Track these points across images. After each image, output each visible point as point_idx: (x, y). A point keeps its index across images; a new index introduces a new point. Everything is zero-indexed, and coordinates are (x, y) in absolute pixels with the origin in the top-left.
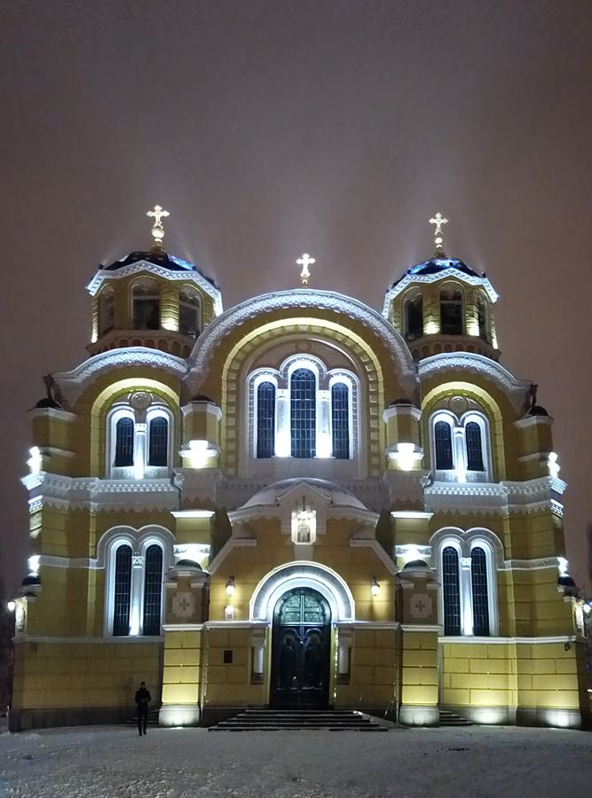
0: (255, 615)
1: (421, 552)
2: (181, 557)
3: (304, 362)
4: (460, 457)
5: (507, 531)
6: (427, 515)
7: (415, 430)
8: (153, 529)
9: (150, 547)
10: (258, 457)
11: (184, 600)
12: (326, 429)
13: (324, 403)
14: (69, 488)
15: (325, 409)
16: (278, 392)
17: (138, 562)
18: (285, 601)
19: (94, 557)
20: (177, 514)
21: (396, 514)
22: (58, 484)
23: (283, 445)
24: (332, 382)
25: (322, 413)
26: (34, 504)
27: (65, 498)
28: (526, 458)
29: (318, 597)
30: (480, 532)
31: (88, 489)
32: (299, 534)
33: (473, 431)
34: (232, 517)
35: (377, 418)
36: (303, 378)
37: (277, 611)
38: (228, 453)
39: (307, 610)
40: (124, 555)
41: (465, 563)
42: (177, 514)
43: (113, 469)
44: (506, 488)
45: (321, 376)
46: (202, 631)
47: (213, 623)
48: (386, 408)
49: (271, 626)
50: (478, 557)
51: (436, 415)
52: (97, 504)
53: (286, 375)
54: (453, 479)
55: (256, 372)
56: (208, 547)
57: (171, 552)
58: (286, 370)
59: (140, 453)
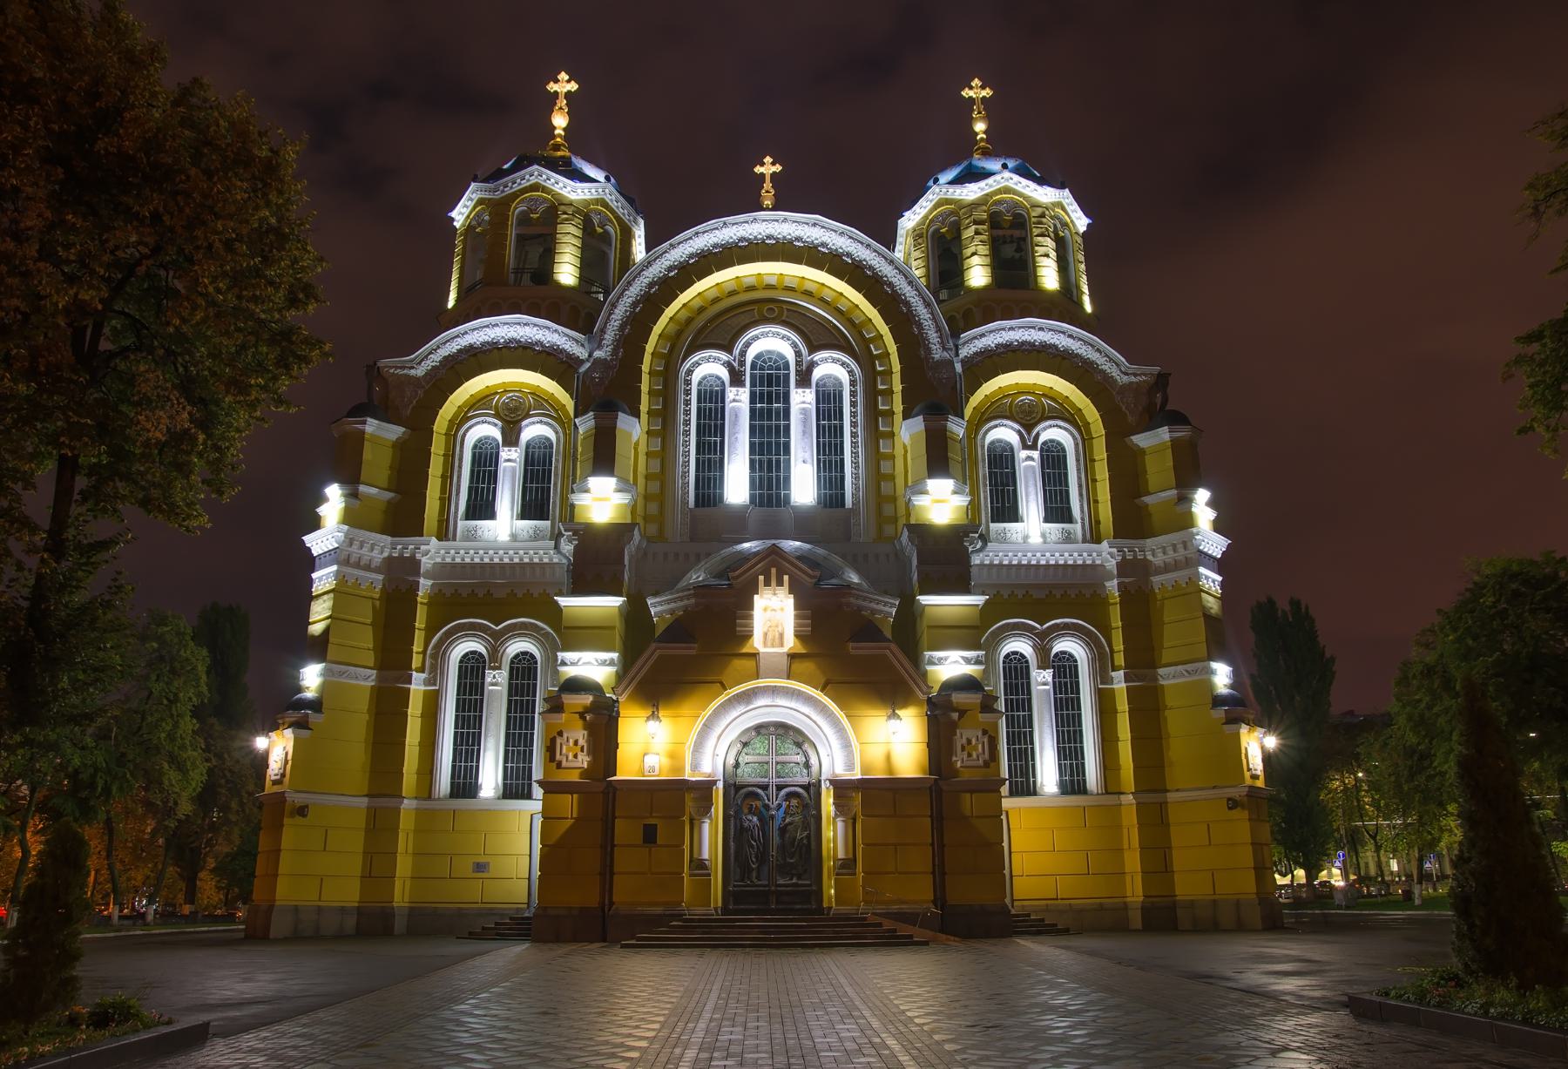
1: (968, 661)
2: (570, 672)
4: (1031, 505)
5: (1116, 622)
6: (977, 600)
7: (955, 455)
9: (517, 656)
10: (697, 504)
11: (576, 743)
12: (807, 456)
13: (805, 412)
14: (386, 554)
15: (805, 422)
16: (731, 393)
17: (497, 681)
18: (745, 744)
19: (421, 670)
20: (564, 601)
21: (926, 600)
22: (367, 547)
23: (737, 487)
24: (817, 373)
25: (800, 428)
26: (320, 579)
27: (377, 570)
28: (1146, 499)
30: (1066, 626)
31: (418, 556)
32: (766, 634)
33: (1053, 459)
34: (656, 607)
35: (892, 435)
36: (770, 368)
37: (731, 761)
38: (647, 498)
40: (473, 670)
41: (1042, 678)
42: (564, 601)
43: (462, 525)
44: (1115, 550)
45: (798, 363)
48: (906, 415)
49: (720, 785)
50: (1064, 668)
51: (996, 426)
52: (430, 583)
53: (742, 363)
54: (1020, 540)
55: (696, 358)
56: (615, 655)
57: (553, 664)
58: (743, 353)
59: (506, 500)
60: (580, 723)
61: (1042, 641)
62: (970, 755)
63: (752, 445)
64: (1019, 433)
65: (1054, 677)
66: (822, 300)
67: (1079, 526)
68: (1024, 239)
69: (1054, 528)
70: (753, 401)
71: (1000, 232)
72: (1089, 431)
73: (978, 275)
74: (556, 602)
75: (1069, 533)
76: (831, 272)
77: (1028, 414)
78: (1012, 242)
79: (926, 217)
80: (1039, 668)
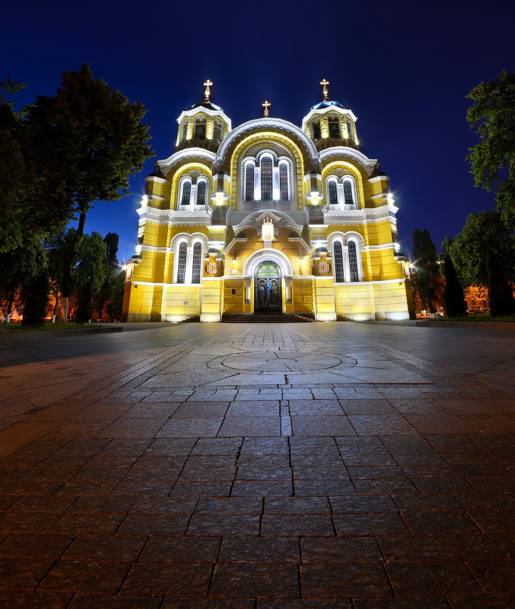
0: (246, 273)
1: (323, 243)
2: (211, 247)
3: (267, 154)
8: (198, 235)
10: (246, 200)
11: (213, 267)
12: (277, 186)
15: (277, 177)
16: (256, 169)
18: (260, 267)
25: (275, 178)
29: (275, 265)
33: (347, 187)
35: (301, 180)
37: (256, 272)
39: (270, 271)
41: (345, 249)
45: (274, 160)
46: (221, 281)
47: (227, 276)
48: (305, 174)
49: (253, 278)
53: (259, 160)
54: (338, 209)
58: (259, 158)
60: (214, 261)
61: (345, 238)
62: (324, 269)
63: (262, 183)
64: (337, 179)
65: (349, 248)
66: (281, 142)
67: (355, 205)
68: (338, 124)
69: (348, 206)
70: (262, 171)
71: (331, 122)
72: (357, 178)
73: (325, 134)
74: (207, 228)
75: (352, 207)
76: (284, 134)
77: (340, 173)
78: (335, 125)
79: (310, 118)
80: (344, 245)
